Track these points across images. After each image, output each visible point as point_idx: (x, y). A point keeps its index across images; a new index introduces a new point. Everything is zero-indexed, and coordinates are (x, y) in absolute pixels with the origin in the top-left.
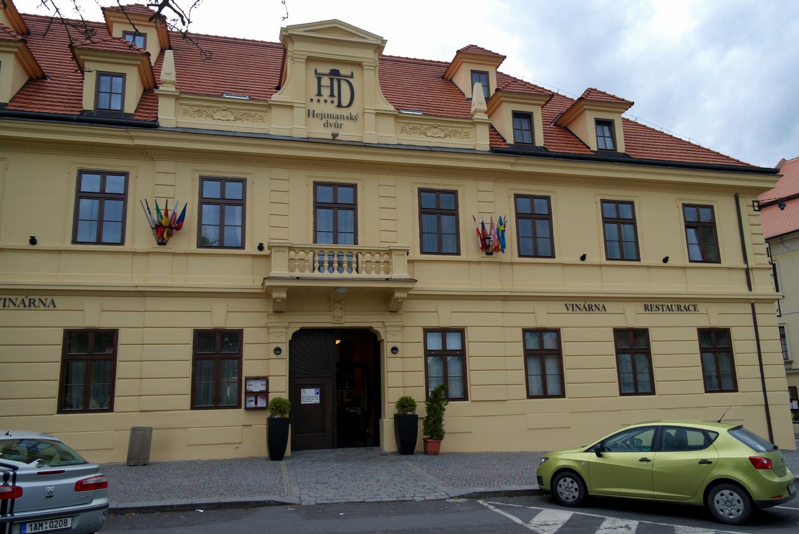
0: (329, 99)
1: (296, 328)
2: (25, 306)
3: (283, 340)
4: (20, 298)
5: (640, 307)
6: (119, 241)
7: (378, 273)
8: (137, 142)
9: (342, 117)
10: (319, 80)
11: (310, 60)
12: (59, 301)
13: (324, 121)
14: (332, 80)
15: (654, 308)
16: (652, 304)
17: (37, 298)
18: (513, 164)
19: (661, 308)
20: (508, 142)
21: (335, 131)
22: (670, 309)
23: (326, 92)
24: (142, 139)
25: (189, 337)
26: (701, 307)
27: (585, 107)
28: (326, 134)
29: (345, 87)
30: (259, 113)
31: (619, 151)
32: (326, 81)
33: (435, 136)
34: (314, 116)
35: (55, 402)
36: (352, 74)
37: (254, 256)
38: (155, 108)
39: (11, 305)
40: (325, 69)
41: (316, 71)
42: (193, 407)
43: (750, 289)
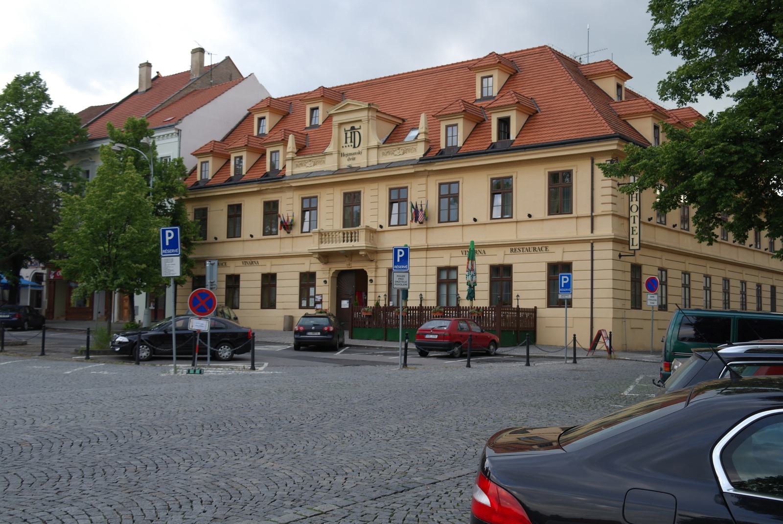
1: (333, 270)
9: (355, 154)
10: (346, 134)
14: (351, 133)
15: (518, 250)
16: (515, 247)
19: (521, 250)
23: (349, 140)
29: (357, 134)
32: (349, 135)
35: (259, 304)
40: (348, 127)
43: (592, 232)
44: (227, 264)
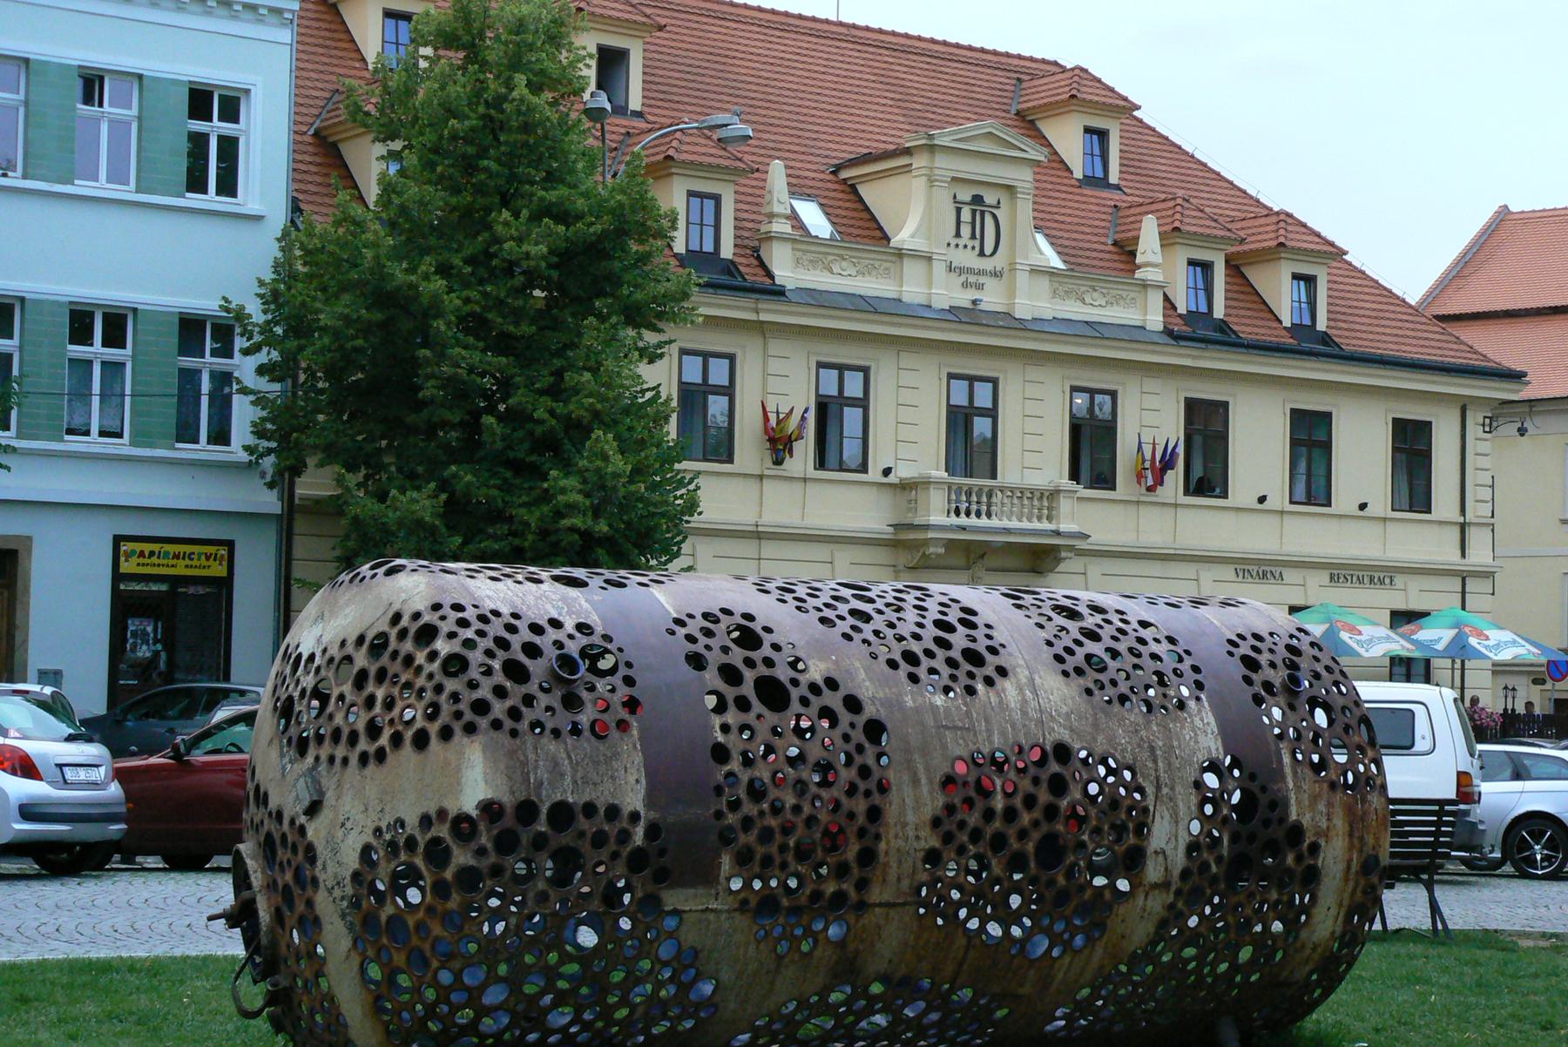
5: (1324, 577)
8: (763, 317)
9: (981, 273)
10: (959, 211)
13: (963, 278)
14: (974, 212)
16: (1341, 573)
18: (1195, 357)
20: (1179, 311)
21: (977, 295)
22: (1360, 581)
23: (966, 231)
26: (1399, 580)
29: (989, 221)
30: (888, 265)
32: (966, 215)
40: (965, 195)
41: (955, 197)
43: (1463, 555)
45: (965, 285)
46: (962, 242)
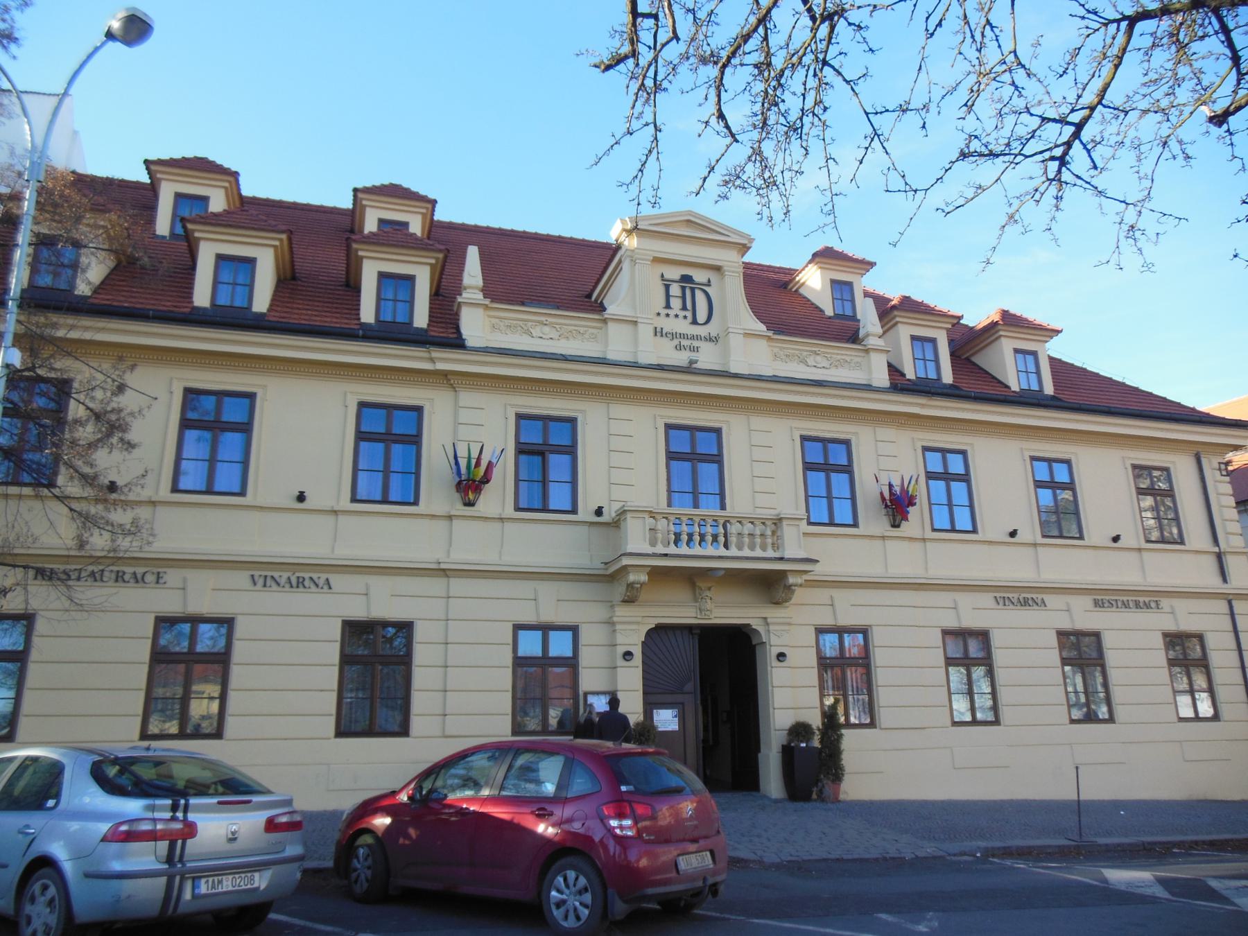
0: (682, 314)
2: (292, 587)
3: (633, 638)
4: (285, 575)
5: (1087, 601)
6: (237, 490)
7: (752, 548)
8: (441, 366)
9: (698, 338)
10: (667, 287)
11: (657, 260)
12: (335, 579)
13: (676, 342)
14: (683, 289)
16: (1105, 598)
17: (307, 575)
18: (923, 406)
20: (908, 377)
22: (1126, 605)
23: (676, 303)
24: (446, 360)
25: (336, 632)
26: (1165, 603)
27: (1001, 333)
28: (681, 358)
29: (700, 297)
30: (591, 330)
31: (1046, 393)
32: (675, 290)
33: (819, 366)
34: (662, 336)
36: (709, 281)
37: (592, 524)
38: (355, 307)
39: (274, 584)
40: (674, 273)
42: (341, 733)
43: (1225, 580)
44: (166, 578)
45: (679, 348)
46: (672, 313)
